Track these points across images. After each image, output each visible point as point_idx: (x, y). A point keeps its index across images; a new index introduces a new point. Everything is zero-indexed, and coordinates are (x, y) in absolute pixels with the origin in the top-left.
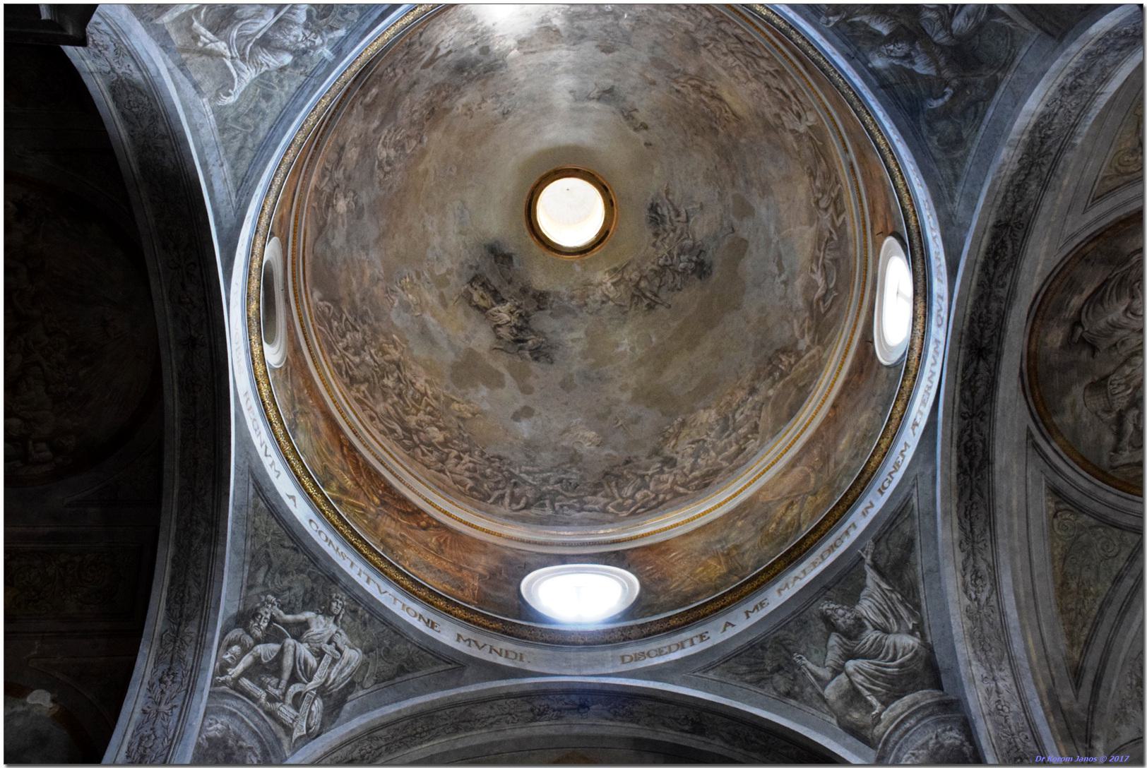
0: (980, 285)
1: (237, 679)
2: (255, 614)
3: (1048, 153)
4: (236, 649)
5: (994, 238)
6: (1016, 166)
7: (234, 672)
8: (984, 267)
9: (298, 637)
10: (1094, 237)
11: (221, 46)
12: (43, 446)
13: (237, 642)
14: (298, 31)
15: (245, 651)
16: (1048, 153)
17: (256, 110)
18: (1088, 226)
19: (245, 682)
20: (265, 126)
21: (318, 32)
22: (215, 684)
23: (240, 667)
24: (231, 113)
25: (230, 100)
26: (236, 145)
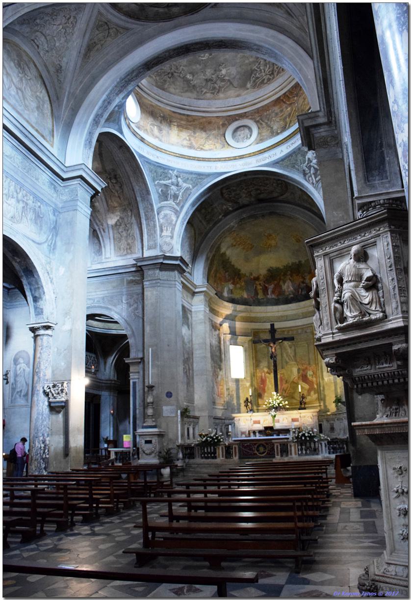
0: (167, 60)
1: (316, 181)
2: (304, 171)
3: (126, 81)
4: (310, 178)
5: (152, 67)
6: (132, 83)
7: (314, 182)
8: (162, 63)
9: (311, 162)
10: (138, 19)
11: (180, 194)
13: (309, 177)
14: (173, 180)
15: (311, 176)
16: (126, 81)
17: (192, 180)
18: (137, 24)
20: (194, 176)
21: (172, 176)
22: (315, 187)
23: (314, 179)
24: (194, 185)
25: (191, 186)
26: (200, 180)
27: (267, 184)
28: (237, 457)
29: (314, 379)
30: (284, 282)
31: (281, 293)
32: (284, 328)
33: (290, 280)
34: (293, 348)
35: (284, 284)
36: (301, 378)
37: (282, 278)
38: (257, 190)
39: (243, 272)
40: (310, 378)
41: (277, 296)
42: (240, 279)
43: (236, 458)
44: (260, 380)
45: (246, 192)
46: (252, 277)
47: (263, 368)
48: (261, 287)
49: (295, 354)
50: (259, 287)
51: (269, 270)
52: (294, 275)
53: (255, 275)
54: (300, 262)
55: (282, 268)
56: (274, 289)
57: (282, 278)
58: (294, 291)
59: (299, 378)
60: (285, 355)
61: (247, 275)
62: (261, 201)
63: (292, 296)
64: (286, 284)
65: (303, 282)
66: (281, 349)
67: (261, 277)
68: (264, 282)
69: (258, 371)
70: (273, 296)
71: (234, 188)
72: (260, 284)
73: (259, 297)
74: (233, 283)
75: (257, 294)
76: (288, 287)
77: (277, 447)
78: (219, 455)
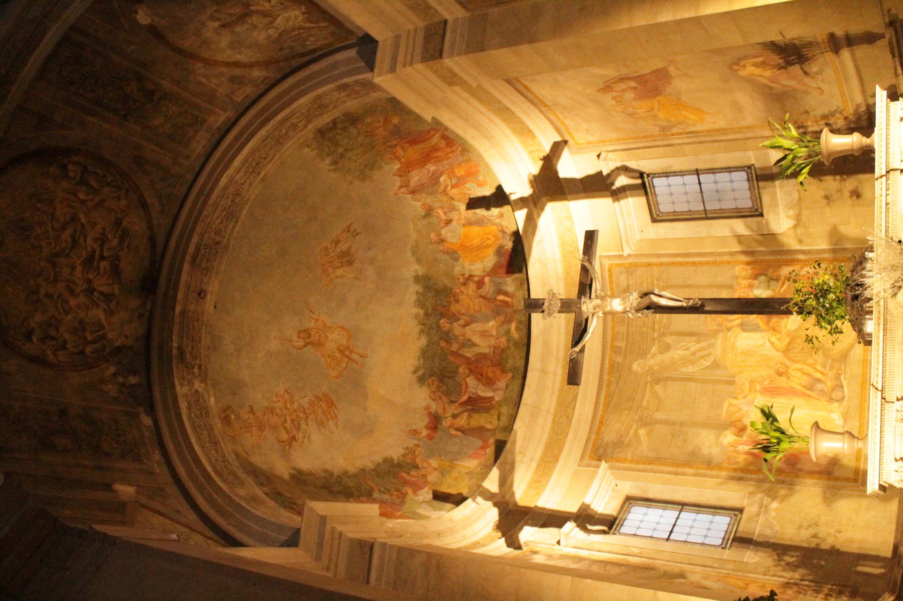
12: (71, 174)
27: (74, 219)
31: (498, 360)
32: (602, 363)
33: (467, 324)
34: (669, 339)
35: (474, 345)
39: (396, 453)
42: (417, 467)
45: (82, 299)
46: (425, 433)
48: (466, 414)
49: (691, 334)
50: (462, 421)
51: (421, 380)
52: (454, 308)
53: (421, 423)
54: (417, 279)
55: (424, 341)
57: (455, 347)
58: (502, 318)
60: (690, 369)
61: (411, 443)
63: (513, 325)
64: (476, 339)
65: (480, 284)
66: (667, 379)
67: (434, 407)
68: (452, 402)
71: (39, 318)
72: (455, 416)
73: (489, 426)
74: (416, 488)
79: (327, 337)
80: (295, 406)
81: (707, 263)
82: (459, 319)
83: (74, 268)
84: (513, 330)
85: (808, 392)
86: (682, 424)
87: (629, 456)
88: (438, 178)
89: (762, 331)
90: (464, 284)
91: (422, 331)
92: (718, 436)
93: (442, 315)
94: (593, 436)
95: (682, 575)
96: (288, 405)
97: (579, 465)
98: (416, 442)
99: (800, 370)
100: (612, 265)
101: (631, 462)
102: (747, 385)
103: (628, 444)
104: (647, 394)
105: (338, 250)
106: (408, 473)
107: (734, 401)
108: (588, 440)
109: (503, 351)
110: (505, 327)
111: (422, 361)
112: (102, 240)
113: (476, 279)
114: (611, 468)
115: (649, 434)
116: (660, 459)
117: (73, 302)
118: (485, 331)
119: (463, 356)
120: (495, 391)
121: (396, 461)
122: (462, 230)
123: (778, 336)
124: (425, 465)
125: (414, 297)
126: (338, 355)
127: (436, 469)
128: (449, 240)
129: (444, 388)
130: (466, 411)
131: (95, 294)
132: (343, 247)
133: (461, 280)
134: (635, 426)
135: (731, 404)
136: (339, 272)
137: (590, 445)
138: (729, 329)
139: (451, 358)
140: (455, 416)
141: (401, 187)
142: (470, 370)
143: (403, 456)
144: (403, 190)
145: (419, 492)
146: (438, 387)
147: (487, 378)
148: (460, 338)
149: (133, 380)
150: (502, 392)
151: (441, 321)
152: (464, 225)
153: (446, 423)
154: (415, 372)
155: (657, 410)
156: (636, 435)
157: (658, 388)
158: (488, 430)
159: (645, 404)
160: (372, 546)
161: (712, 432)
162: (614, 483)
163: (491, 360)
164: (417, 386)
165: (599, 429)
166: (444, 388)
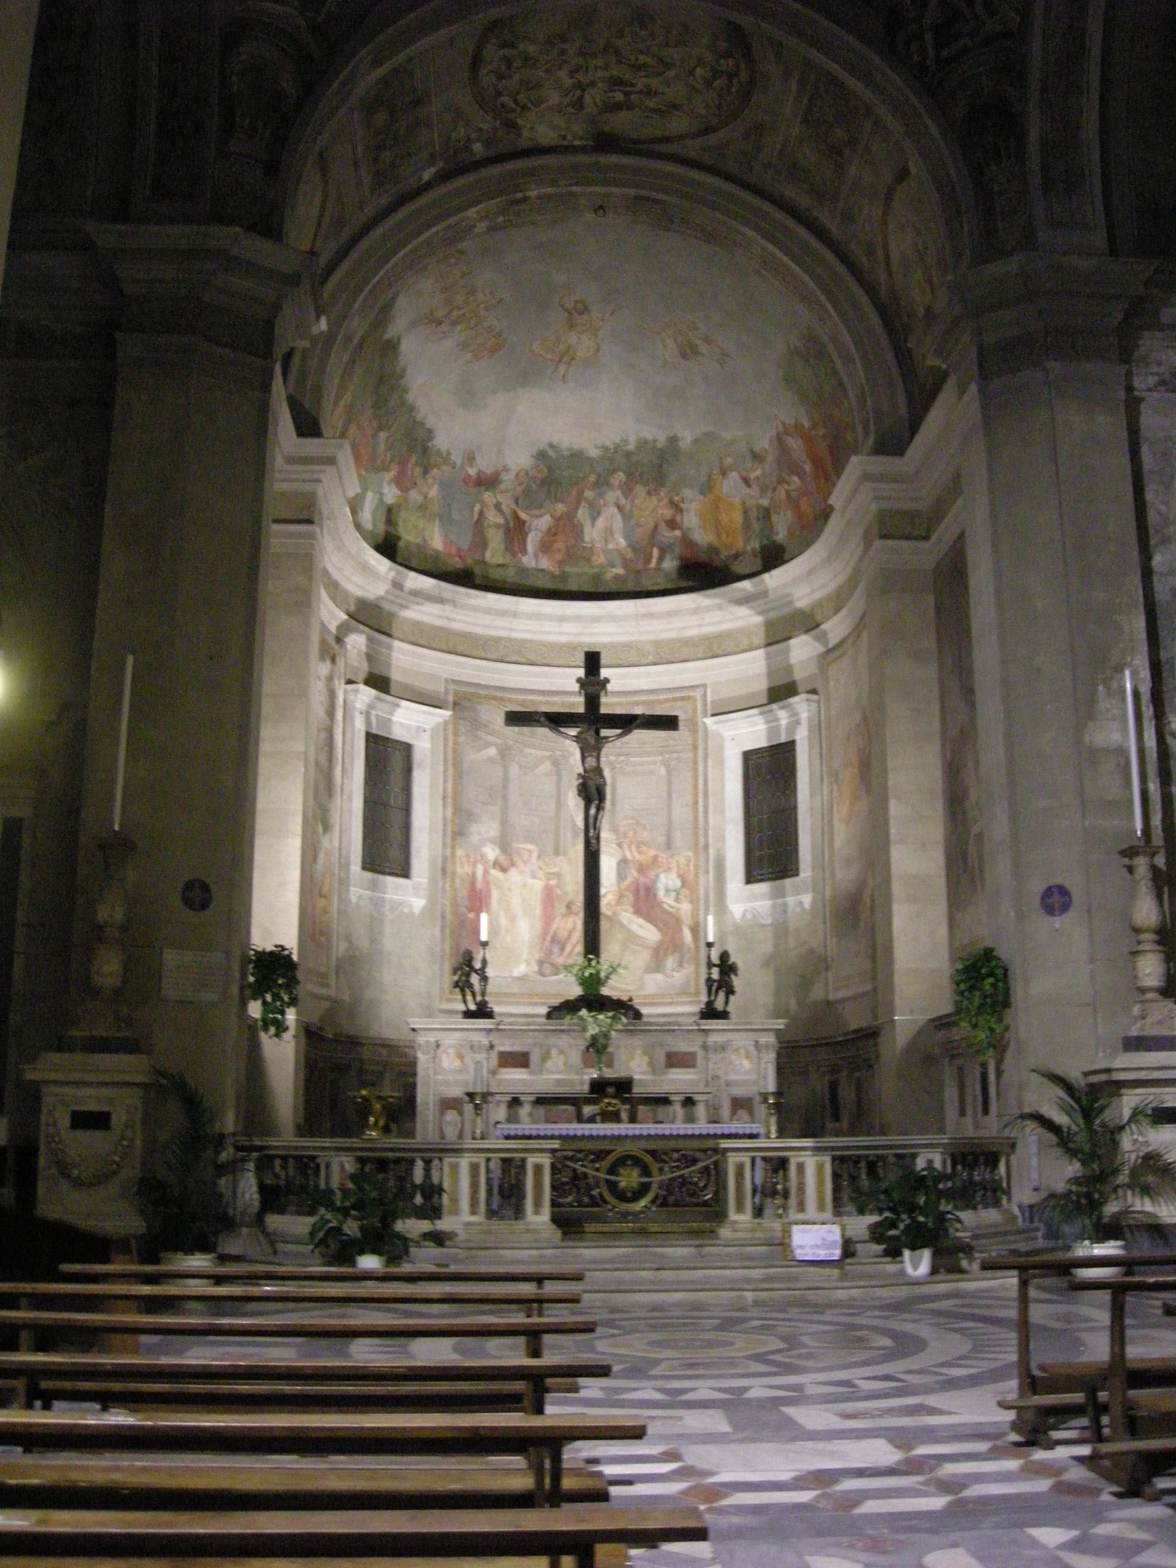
4: (913, 47)
19: (945, 54)
23: (931, 52)
27: (667, 66)
28: (545, 1215)
29: (685, 908)
30: (595, 515)
31: (577, 552)
33: (620, 508)
35: (594, 520)
36: (630, 897)
37: (589, 494)
38: (617, 82)
39: (441, 442)
40: (668, 901)
41: (561, 562)
42: (426, 472)
43: (539, 1218)
44: (463, 892)
45: (567, 82)
46: (472, 472)
47: (484, 841)
48: (501, 521)
50: (493, 517)
51: (541, 456)
52: (640, 491)
53: (485, 465)
54: (673, 440)
55: (594, 453)
56: (552, 533)
57: (589, 494)
58: (630, 555)
59: (621, 896)
61: (457, 458)
62: (606, 143)
64: (601, 522)
65: (672, 524)
66: (559, 775)
67: (507, 478)
68: (517, 501)
69: (459, 852)
70: (545, 563)
71: (532, 49)
72: (498, 507)
73: (488, 554)
74: (401, 481)
75: (481, 543)
76: (608, 532)
77: (740, 1175)
78: (455, 1200)
79: (582, 332)
80: (482, 313)
81: (696, 818)
82: (626, 498)
83: (606, 68)
84: (615, 571)
85: (549, 938)
86: (505, 798)
87: (461, 739)
88: (798, 474)
89: (619, 884)
90: (671, 502)
91: (605, 449)
92: (493, 841)
93: (629, 475)
94: (483, 692)
95: (327, 827)
96: (482, 306)
97: (446, 680)
98: (459, 463)
99: (574, 928)
100: (695, 700)
101: (455, 743)
102: (555, 870)
103: (476, 736)
104: (539, 753)
105: (698, 342)
106: (416, 464)
107: (535, 856)
108: (478, 685)
109: (588, 560)
110: (618, 561)
111: (566, 453)
112: (649, 92)
113: (678, 519)
114: (446, 722)
115: (490, 760)
116: (460, 777)
117: (563, 74)
118: (612, 535)
119: (577, 508)
120: (536, 555)
121: (430, 444)
122: (737, 501)
123: (613, 903)
124: (430, 481)
125: (650, 437)
126: (562, 348)
127: (425, 497)
128: (725, 482)
129: (534, 487)
130: (506, 520)
131: (578, 93)
132: (703, 348)
133: (676, 498)
134: (499, 741)
135: (530, 852)
136: (670, 343)
137: (472, 690)
138: (619, 845)
139: (574, 493)
140: (498, 507)
141: (784, 424)
142: (560, 518)
143: (439, 453)
144: (781, 428)
145: (393, 486)
146: (534, 479)
147: (552, 543)
148: (602, 501)
149: (477, 147)
150: (533, 564)
151: (621, 474)
152: (744, 503)
153: (488, 496)
154: (551, 445)
155: (520, 766)
156: (488, 745)
157: (547, 766)
158: (483, 554)
159: (527, 750)
160: (310, 522)
161: (497, 834)
162: (427, 727)
163: (575, 545)
164: (534, 451)
165: (495, 698)
166: (534, 487)
